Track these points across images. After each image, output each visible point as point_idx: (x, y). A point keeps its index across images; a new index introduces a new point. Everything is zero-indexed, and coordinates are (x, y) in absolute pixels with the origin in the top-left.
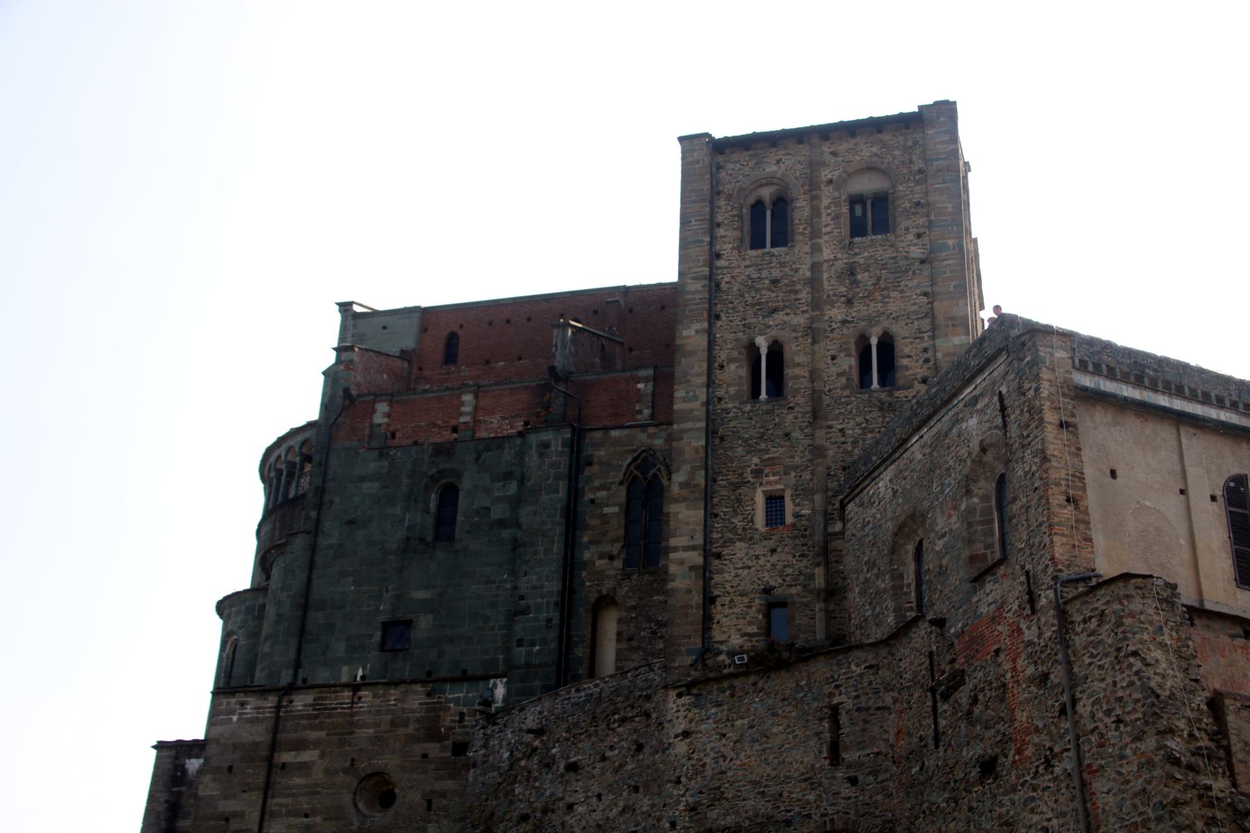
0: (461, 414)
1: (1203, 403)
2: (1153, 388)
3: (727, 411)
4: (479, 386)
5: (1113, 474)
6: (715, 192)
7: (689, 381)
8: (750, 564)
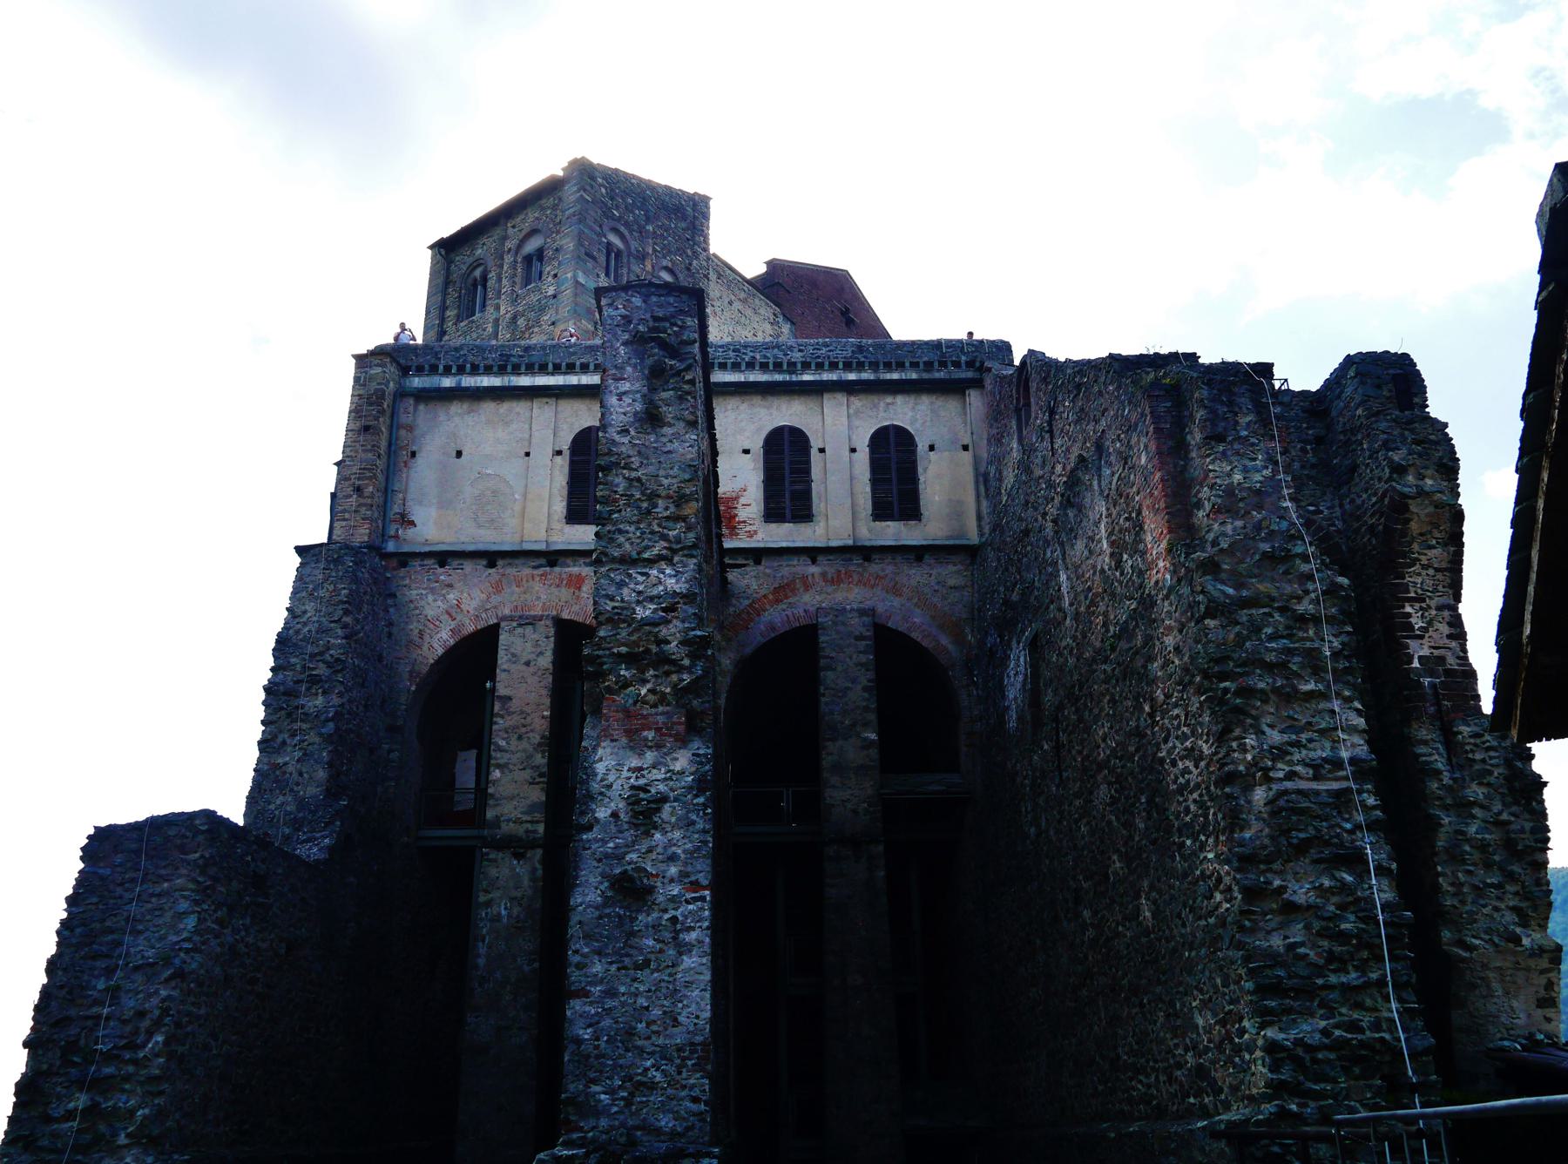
1: (565, 373)
2: (516, 371)
5: (459, 454)
6: (447, 283)
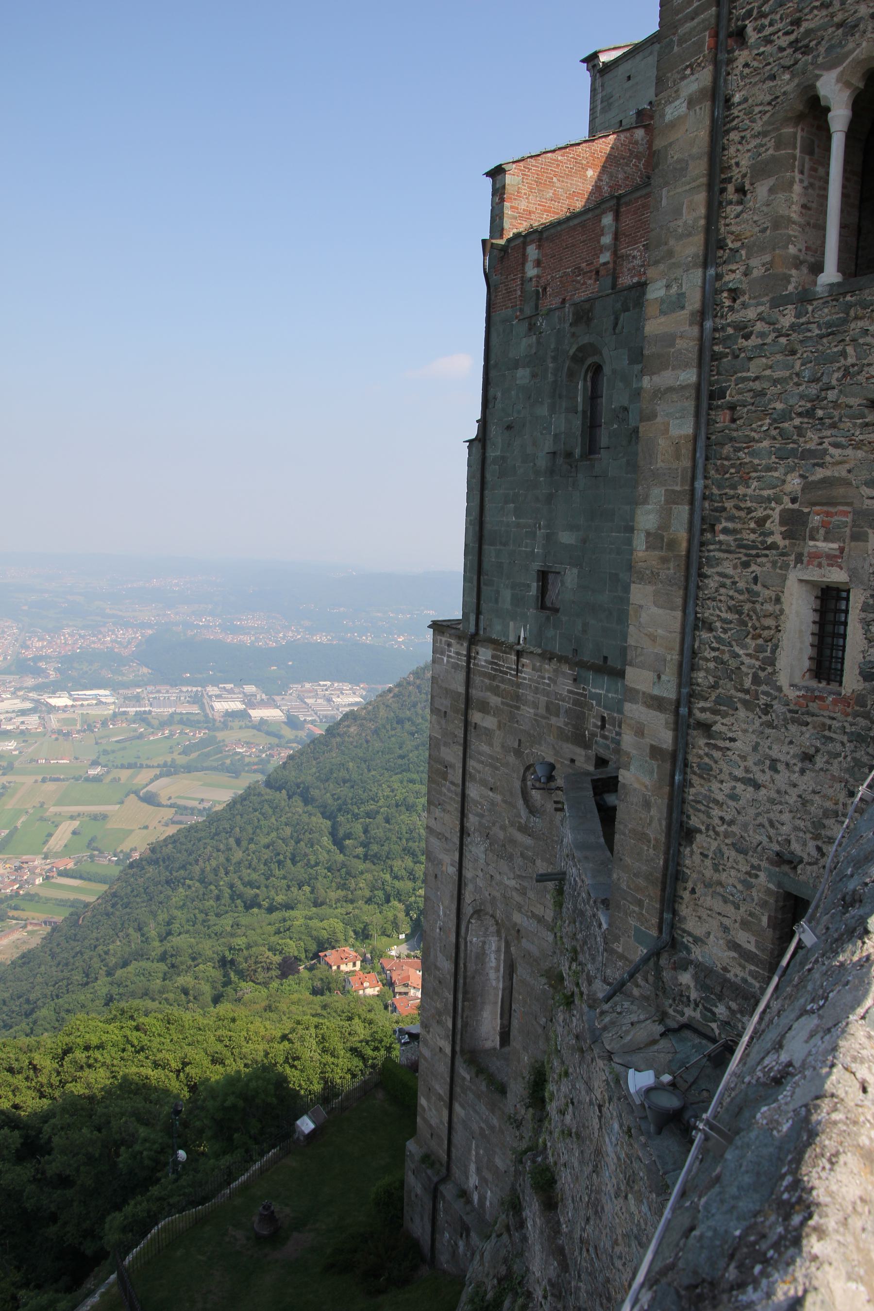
0: (602, 249)
3: (744, 330)
4: (619, 198)
7: (670, 254)
8: (761, 778)
